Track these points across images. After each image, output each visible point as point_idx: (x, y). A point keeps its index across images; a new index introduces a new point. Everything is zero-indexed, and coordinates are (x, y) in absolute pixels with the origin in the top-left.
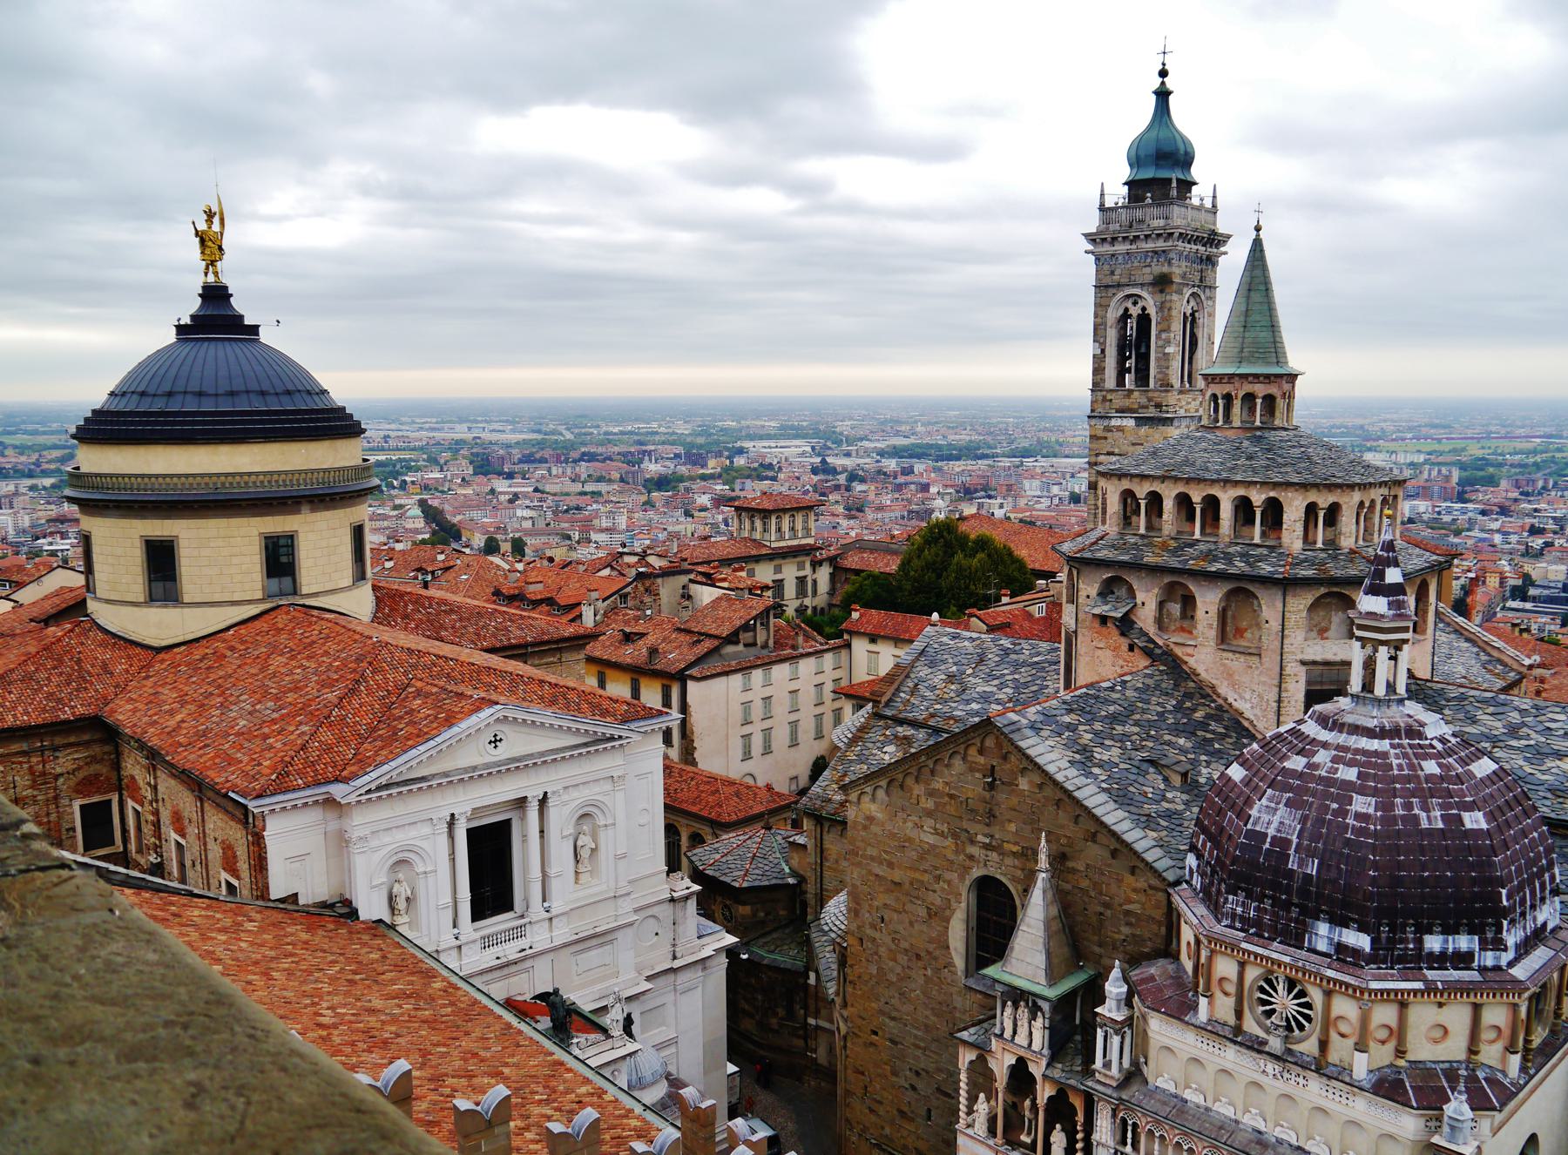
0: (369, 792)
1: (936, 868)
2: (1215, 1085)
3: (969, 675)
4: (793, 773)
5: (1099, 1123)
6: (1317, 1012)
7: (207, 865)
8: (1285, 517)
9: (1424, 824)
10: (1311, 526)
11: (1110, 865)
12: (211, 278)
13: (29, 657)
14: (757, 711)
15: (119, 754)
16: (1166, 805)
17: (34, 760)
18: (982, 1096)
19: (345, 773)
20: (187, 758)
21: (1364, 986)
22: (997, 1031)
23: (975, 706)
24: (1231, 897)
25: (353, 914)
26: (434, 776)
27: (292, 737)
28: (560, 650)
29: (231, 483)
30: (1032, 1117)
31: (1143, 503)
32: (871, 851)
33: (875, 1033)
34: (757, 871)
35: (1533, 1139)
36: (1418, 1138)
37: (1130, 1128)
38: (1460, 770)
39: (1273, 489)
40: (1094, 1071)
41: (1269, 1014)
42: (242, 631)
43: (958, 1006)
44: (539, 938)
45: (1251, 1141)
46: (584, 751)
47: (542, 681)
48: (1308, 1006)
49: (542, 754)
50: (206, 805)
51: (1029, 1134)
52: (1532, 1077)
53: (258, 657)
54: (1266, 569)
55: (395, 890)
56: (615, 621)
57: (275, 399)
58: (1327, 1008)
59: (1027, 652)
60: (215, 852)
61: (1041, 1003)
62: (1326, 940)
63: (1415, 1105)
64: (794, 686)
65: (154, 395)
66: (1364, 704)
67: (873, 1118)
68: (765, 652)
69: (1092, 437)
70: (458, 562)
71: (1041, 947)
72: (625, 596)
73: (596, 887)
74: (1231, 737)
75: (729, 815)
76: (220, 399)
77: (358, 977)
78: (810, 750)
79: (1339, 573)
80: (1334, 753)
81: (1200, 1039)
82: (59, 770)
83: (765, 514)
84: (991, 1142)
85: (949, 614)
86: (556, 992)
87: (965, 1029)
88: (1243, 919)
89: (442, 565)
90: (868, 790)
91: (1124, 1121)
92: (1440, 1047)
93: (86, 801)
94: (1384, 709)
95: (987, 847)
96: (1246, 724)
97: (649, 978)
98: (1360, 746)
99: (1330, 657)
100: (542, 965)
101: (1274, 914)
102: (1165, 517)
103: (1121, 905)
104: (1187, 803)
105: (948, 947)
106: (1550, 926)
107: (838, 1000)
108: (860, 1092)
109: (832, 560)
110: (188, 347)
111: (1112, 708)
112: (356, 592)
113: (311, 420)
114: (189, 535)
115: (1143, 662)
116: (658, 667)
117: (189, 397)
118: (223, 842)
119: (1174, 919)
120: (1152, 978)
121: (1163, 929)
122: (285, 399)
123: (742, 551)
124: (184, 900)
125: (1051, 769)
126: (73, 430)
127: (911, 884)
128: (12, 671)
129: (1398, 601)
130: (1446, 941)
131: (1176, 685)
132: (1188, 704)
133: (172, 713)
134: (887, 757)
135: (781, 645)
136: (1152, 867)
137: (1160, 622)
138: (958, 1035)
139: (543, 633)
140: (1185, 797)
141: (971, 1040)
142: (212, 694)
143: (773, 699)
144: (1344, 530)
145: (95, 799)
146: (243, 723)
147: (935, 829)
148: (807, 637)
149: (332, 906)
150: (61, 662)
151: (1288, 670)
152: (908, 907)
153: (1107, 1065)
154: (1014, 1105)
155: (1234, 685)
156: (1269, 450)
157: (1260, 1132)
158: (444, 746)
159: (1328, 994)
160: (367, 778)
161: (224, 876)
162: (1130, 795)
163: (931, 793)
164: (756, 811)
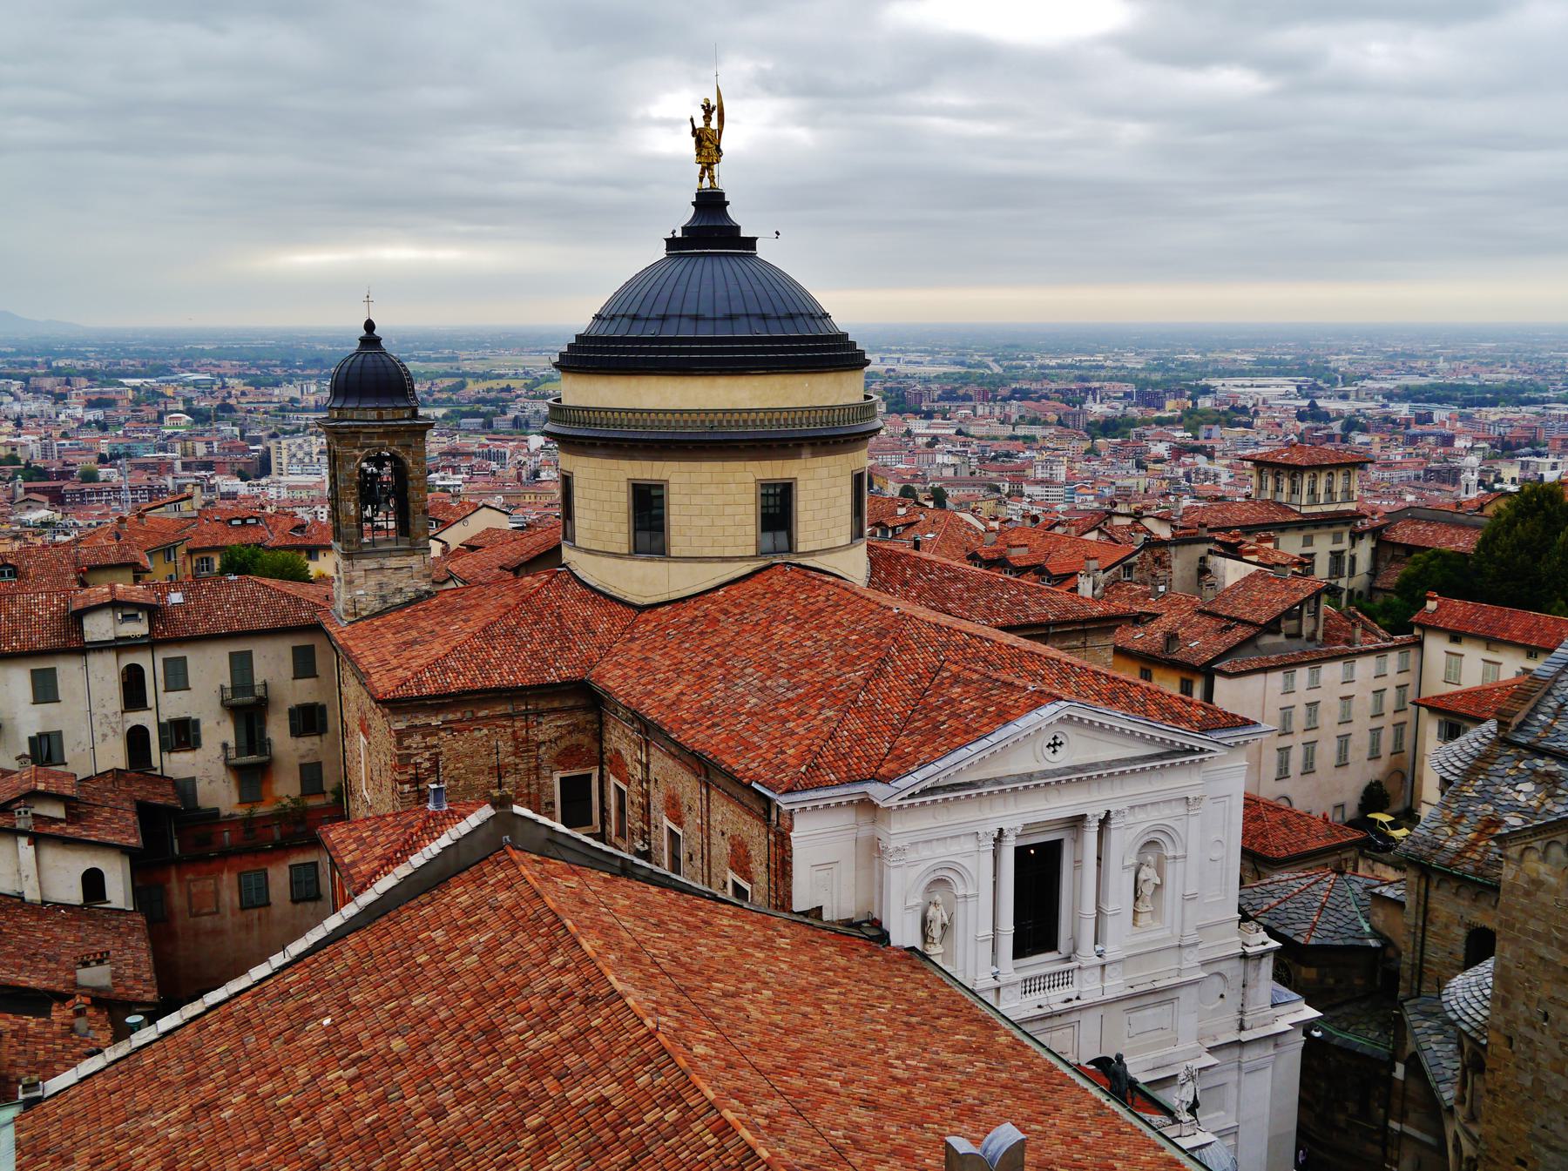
0: (912, 796)
4: (1339, 800)
7: (709, 861)
12: (706, 183)
13: (509, 610)
14: (1299, 718)
15: (602, 724)
17: (518, 724)
19: (882, 771)
20: (696, 738)
25: (884, 937)
26: (984, 782)
27: (816, 722)
28: (1085, 632)
29: (728, 421)
32: (1532, 925)
34: (1327, 926)
42: (733, 593)
44: (1088, 987)
46: (1157, 764)
47: (1096, 673)
49: (1109, 764)
50: (713, 793)
53: (757, 624)
55: (930, 914)
56: (1118, 597)
57: (776, 323)
60: (721, 848)
64: (1347, 690)
65: (647, 319)
68: (1311, 646)
70: (922, 517)
72: (1129, 568)
73: (1157, 932)
75: (1278, 849)
76: (718, 323)
77: (914, 1020)
78: (1362, 773)
82: (541, 738)
83: (1295, 471)
85: (1555, 609)
86: (1119, 1058)
89: (903, 521)
90: (1537, 844)
93: (567, 775)
97: (1212, 1050)
100: (1090, 1021)
107: (1461, 1112)
109: (1376, 532)
110: (679, 266)
112: (853, 552)
113: (816, 349)
114: (677, 476)
116: (1177, 657)
117: (684, 322)
118: (733, 837)
122: (787, 324)
123: (1264, 516)
124: (710, 905)
126: (557, 359)
128: (493, 623)
133: (668, 683)
134: (1522, 798)
135: (1332, 638)
139: (1067, 611)
142: (710, 664)
143: (1321, 705)
145: (576, 772)
146: (754, 701)
148: (1367, 631)
149: (858, 925)
150: (541, 616)
158: (998, 748)
160: (909, 780)
161: (731, 876)
164: (1313, 845)
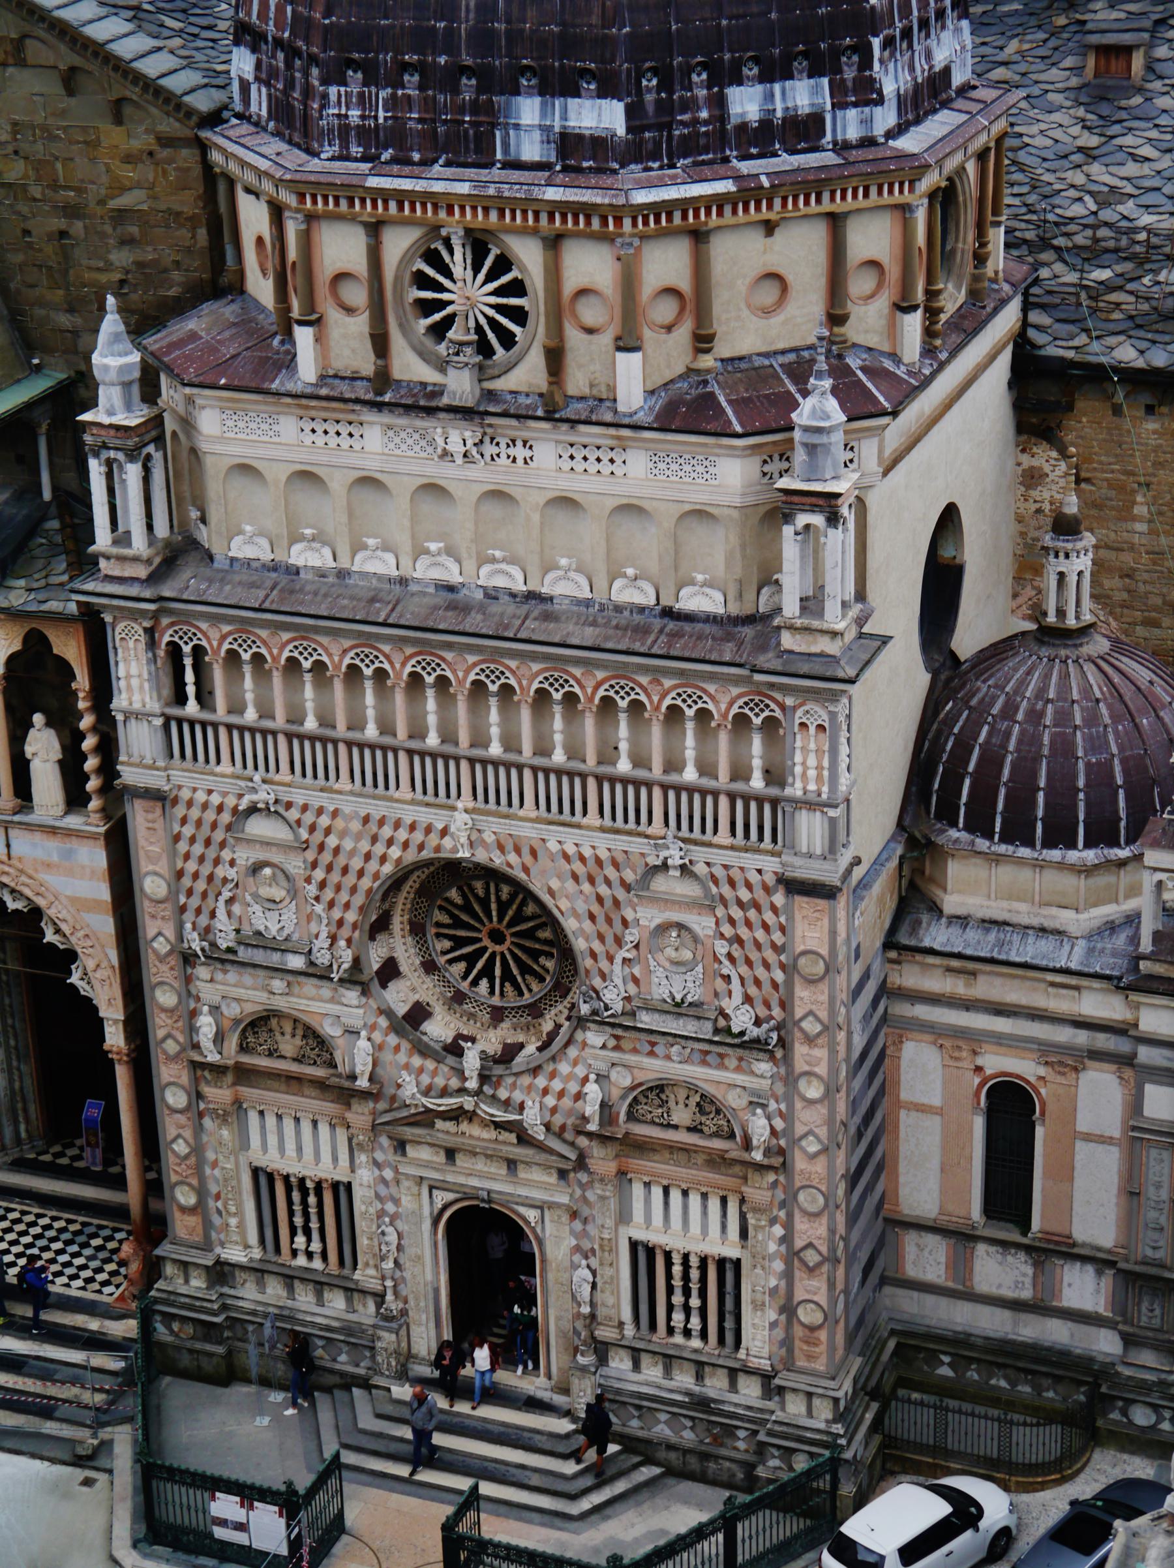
2: (351, 515)
5: (122, 672)
6: (534, 302)
11: (63, 113)
21: (621, 201)
24: (333, 91)
35: (949, 518)
36: (750, 500)
37: (188, 662)
41: (439, 331)
45: (436, 608)
48: (517, 288)
52: (942, 366)
58: (554, 273)
62: (537, 135)
63: (738, 429)
81: (308, 426)
88: (366, 134)
91: (175, 651)
92: (777, 320)
101: (429, 105)
103: (102, 202)
106: (957, 79)
119: (223, 208)
120: (193, 336)
121: (202, 233)
130: (770, 97)
153: (123, 539)
157: (451, 589)
159: (554, 243)
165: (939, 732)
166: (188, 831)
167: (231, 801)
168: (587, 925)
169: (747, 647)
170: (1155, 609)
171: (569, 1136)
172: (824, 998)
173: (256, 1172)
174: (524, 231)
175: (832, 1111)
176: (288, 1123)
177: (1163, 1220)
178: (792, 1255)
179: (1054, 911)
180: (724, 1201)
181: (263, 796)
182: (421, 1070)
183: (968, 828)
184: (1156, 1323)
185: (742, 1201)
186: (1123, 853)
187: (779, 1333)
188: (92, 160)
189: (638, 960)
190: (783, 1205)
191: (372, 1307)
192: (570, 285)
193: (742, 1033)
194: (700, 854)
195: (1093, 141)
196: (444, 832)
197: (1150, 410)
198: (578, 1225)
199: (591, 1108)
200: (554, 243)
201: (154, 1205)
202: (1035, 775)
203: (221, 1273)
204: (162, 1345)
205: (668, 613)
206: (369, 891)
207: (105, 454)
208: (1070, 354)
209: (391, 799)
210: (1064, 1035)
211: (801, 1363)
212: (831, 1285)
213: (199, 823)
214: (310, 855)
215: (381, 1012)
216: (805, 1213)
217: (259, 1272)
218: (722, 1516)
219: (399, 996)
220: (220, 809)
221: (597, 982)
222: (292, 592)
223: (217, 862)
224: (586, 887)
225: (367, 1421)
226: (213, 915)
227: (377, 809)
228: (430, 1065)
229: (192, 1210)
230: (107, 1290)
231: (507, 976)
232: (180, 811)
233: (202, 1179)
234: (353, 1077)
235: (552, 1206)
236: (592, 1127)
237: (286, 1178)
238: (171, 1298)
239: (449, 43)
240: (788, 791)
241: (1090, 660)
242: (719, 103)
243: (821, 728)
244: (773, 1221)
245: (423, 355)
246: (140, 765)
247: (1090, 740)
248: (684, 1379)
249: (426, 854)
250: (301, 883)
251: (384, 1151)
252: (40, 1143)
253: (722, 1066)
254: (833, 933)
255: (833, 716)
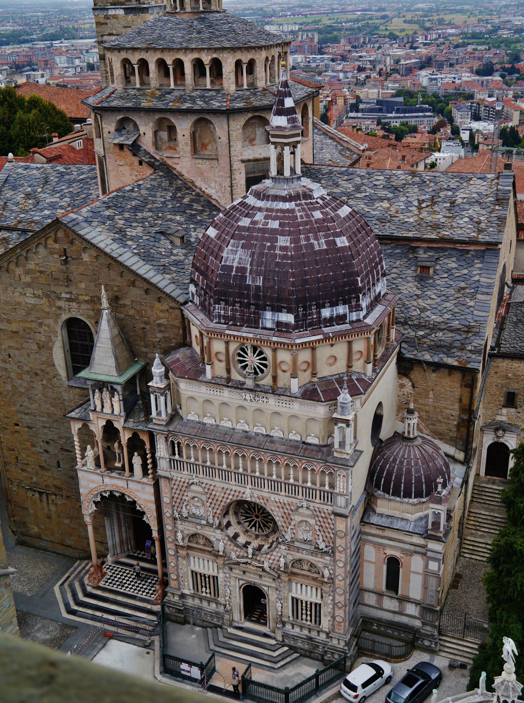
1: (39, 318)
3: (40, 193)
6: (269, 362)
8: (224, 70)
9: (317, 248)
10: (240, 75)
11: (145, 299)
16: (173, 258)
18: (89, 447)
22: (92, 408)
23: (47, 212)
24: (217, 306)
30: (120, 452)
31: (136, 67)
33: (17, 425)
35: (380, 404)
36: (326, 417)
37: (176, 446)
38: (333, 214)
39: (215, 52)
40: (152, 419)
41: (244, 367)
43: (66, 398)
45: (242, 437)
48: (265, 359)
51: (120, 461)
52: (378, 374)
54: (216, 104)
58: (275, 357)
59: (75, 173)
61: (115, 387)
62: (271, 321)
66: (279, 182)
67: (25, 474)
69: (98, 24)
71: (111, 354)
74: (206, 212)
79: (256, 104)
80: (265, 213)
84: (98, 471)
85: (19, 153)
87: (72, 411)
88: (225, 317)
91: (173, 443)
92: (333, 367)
94: (290, 184)
95: (69, 300)
96: (214, 202)
98: (279, 208)
99: (257, 156)
101: (242, 311)
102: (151, 75)
103: (154, 321)
104: (185, 255)
105: (54, 365)
106: (382, 294)
108: (13, 461)
111: (134, 203)
115: (149, 171)
119: (186, 324)
120: (178, 360)
121: (181, 331)
125: (102, 245)
127: (24, 330)
129: (293, 118)
131: (171, 184)
132: (179, 195)
136: (170, 296)
137: (156, 145)
138: (69, 415)
140: (184, 251)
141: (77, 416)
144: (258, 76)
147: (34, 294)
151: (235, 167)
152: (25, 345)
153: (159, 414)
154: (109, 448)
155: (205, 180)
156: (210, 27)
157: (246, 432)
159: (275, 350)
162: (152, 255)
163: (28, 272)
165: (376, 464)
166: (175, 487)
167: (187, 481)
168: (281, 519)
169: (325, 454)
170: (434, 421)
171: (276, 570)
172: (344, 542)
173: (192, 572)
174: (267, 346)
175: (346, 569)
176: (201, 560)
177: (433, 595)
178: (335, 604)
179: (406, 514)
180: (317, 589)
181: (195, 480)
182: (237, 551)
183: (383, 491)
184: (431, 620)
185: (322, 590)
186: (424, 500)
187: (331, 623)
188: (152, 311)
189: (295, 529)
190: (332, 591)
191: (223, 608)
192: (279, 360)
193: (322, 549)
194: (311, 504)
195: (419, 293)
196: (244, 493)
197: (434, 371)
198: (278, 592)
199: (282, 565)
200: (275, 350)
201: (165, 570)
202: (401, 479)
203: (183, 596)
204: (167, 614)
205: (304, 443)
206: (223, 506)
207: (155, 394)
208: (412, 357)
209: (229, 484)
210: (408, 547)
211: (336, 631)
212: (345, 612)
213: (178, 485)
214: (208, 496)
215: (226, 536)
216: (338, 594)
217: (193, 596)
218: (315, 674)
219: (231, 532)
220: (184, 482)
221: (284, 533)
222: (204, 430)
223: (183, 495)
224: (281, 510)
225: (221, 639)
226: (182, 508)
227: (226, 486)
228: (239, 550)
229: (175, 580)
230: (153, 596)
231: (260, 527)
232: (173, 482)
233: (178, 573)
234: (218, 551)
235: (271, 587)
236: (282, 569)
237: (200, 574)
238: (169, 602)
239: (248, 297)
240: (335, 491)
241: (416, 446)
242: (319, 313)
243: (344, 476)
244: (330, 595)
245: (240, 374)
246: (163, 470)
247: (415, 469)
248: (306, 632)
249: (239, 498)
250: (205, 502)
251: (227, 570)
252: (134, 550)
253: (316, 556)
254: (347, 526)
255: (347, 474)
